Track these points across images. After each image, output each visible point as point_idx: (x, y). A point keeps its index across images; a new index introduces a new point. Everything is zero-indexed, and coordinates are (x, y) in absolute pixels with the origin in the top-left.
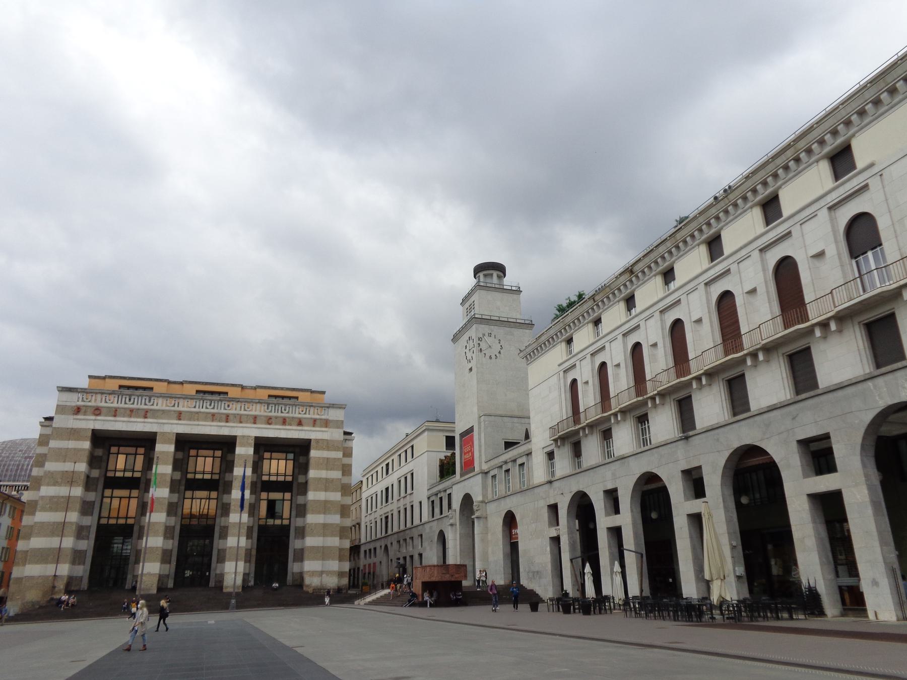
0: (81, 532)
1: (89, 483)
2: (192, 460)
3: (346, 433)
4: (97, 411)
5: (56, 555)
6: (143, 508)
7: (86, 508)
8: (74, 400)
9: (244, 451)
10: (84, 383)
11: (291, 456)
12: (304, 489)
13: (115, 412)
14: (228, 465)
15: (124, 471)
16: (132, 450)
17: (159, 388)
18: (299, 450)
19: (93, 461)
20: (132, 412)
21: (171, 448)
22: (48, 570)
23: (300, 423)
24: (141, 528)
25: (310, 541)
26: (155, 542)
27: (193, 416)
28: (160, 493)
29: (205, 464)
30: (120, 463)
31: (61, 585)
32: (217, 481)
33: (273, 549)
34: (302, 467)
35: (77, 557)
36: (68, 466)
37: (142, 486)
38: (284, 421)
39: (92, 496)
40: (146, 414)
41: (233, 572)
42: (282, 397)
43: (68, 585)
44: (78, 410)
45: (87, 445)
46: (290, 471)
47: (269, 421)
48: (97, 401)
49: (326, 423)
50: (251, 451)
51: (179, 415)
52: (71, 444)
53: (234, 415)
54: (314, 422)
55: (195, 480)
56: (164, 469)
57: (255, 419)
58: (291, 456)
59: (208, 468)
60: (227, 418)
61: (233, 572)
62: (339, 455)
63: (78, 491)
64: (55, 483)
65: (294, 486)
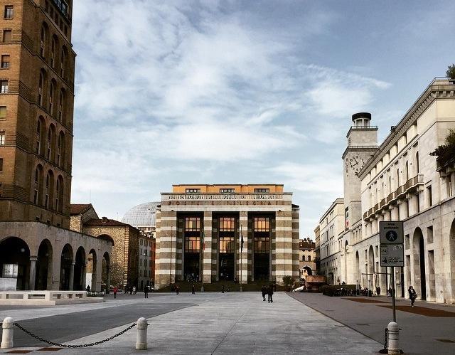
0: (178, 256)
1: (178, 235)
2: (221, 223)
3: (293, 206)
4: (178, 203)
5: (169, 266)
6: (202, 246)
7: (178, 246)
8: (167, 198)
9: (243, 219)
10: (171, 191)
11: (268, 219)
12: (274, 236)
13: (185, 203)
14: (237, 225)
15: (193, 229)
16: (194, 219)
17: (203, 190)
18: (271, 216)
19: (179, 225)
20: (193, 203)
21: (211, 219)
22: (167, 272)
23: (269, 204)
24: (202, 255)
25: (278, 262)
26: (207, 261)
27: (219, 203)
28: (208, 239)
29: (227, 225)
30: (190, 225)
31: (173, 278)
32: (233, 232)
33: (262, 264)
34: (273, 225)
35: (178, 267)
36: (169, 228)
37: (201, 235)
38: (262, 203)
39: (181, 241)
40: (198, 203)
41: (243, 275)
42: (260, 190)
43: (176, 278)
44: (170, 203)
45: (175, 218)
46: (268, 227)
47: (254, 203)
48: (177, 198)
49: (283, 203)
50: (246, 218)
51: (213, 203)
52: (169, 218)
53: (238, 202)
54: (277, 203)
55: (223, 232)
56: (208, 228)
57: (247, 203)
58: (268, 219)
59: (229, 227)
60: (234, 203)
61: (243, 275)
62: (290, 219)
63: (174, 239)
64: (166, 236)
65: (270, 235)
